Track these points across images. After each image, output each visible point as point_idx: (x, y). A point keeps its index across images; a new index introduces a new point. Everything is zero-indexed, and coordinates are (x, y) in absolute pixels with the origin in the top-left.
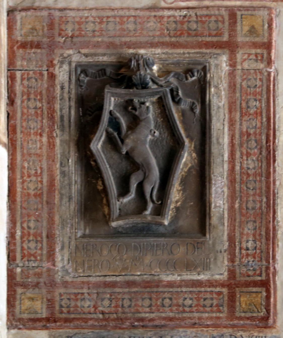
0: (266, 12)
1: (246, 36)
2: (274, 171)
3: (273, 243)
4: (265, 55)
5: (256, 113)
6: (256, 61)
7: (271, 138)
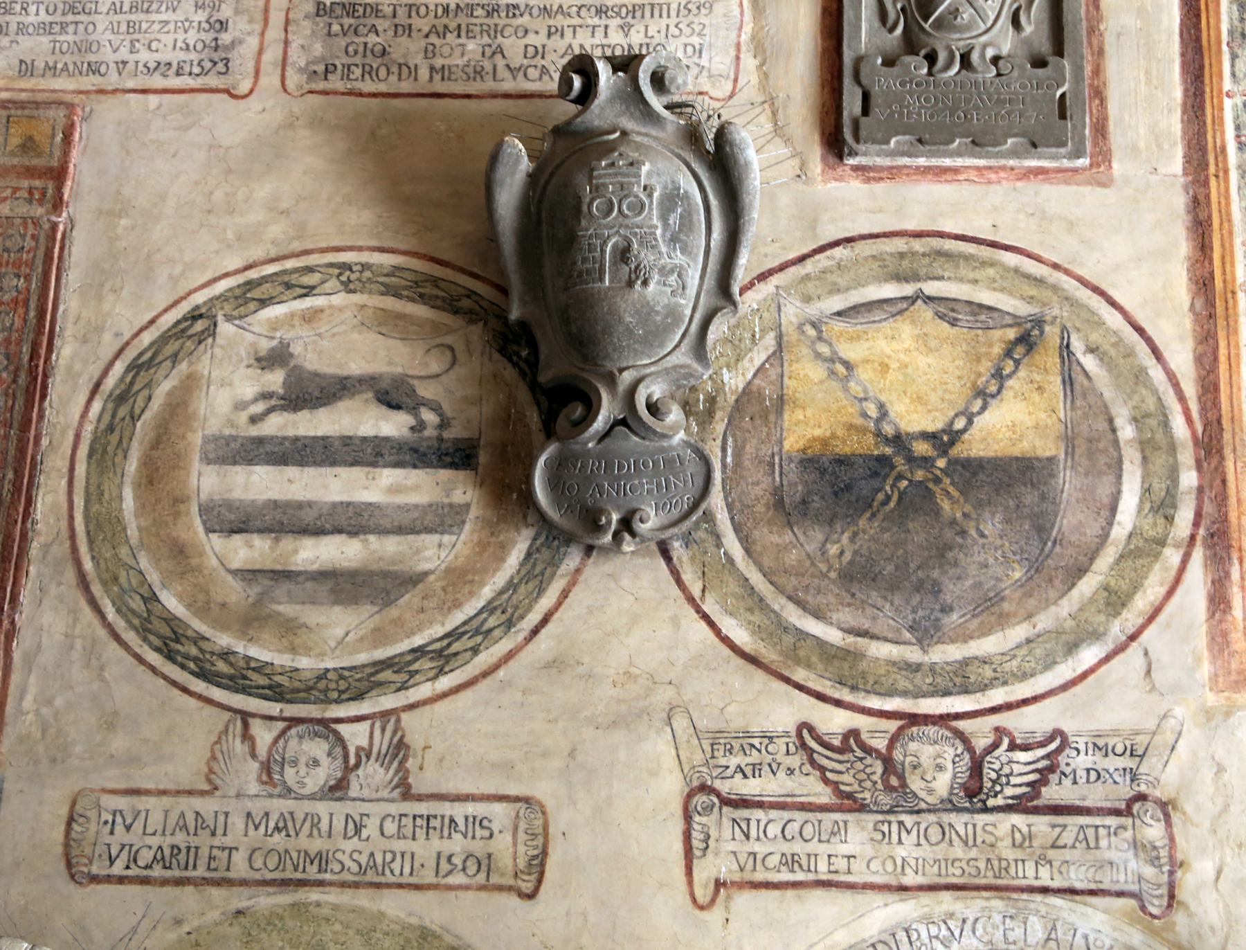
0: (62, 113)
1: (13, 154)
2: (41, 416)
3: (17, 568)
4: (50, 192)
5: (15, 301)
6: (30, 201)
7: (43, 352)
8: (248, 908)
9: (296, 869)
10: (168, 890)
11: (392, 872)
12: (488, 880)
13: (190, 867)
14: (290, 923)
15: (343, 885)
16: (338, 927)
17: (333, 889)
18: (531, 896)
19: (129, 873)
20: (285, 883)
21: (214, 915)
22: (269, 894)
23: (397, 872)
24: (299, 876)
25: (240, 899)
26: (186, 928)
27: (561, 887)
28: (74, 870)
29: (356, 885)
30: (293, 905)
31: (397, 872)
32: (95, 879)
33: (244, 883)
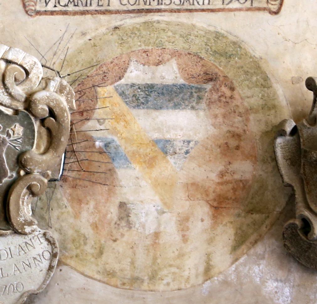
8: (121, 25)
9: (145, 4)
10: (77, 17)
11: (198, 3)
12: (252, 5)
13: (88, 5)
14: (144, 33)
15: (172, 11)
16: (170, 34)
17: (166, 13)
18: (276, 13)
19: (56, 9)
20: (140, 11)
21: (103, 30)
22: (131, 18)
23: (201, 3)
24: (147, 7)
25: (116, 21)
26: (88, 37)
27: (294, 7)
28: (27, 9)
29: (179, 11)
30: (145, 23)
31: (201, 3)
32: (38, 13)
33: (117, 12)
